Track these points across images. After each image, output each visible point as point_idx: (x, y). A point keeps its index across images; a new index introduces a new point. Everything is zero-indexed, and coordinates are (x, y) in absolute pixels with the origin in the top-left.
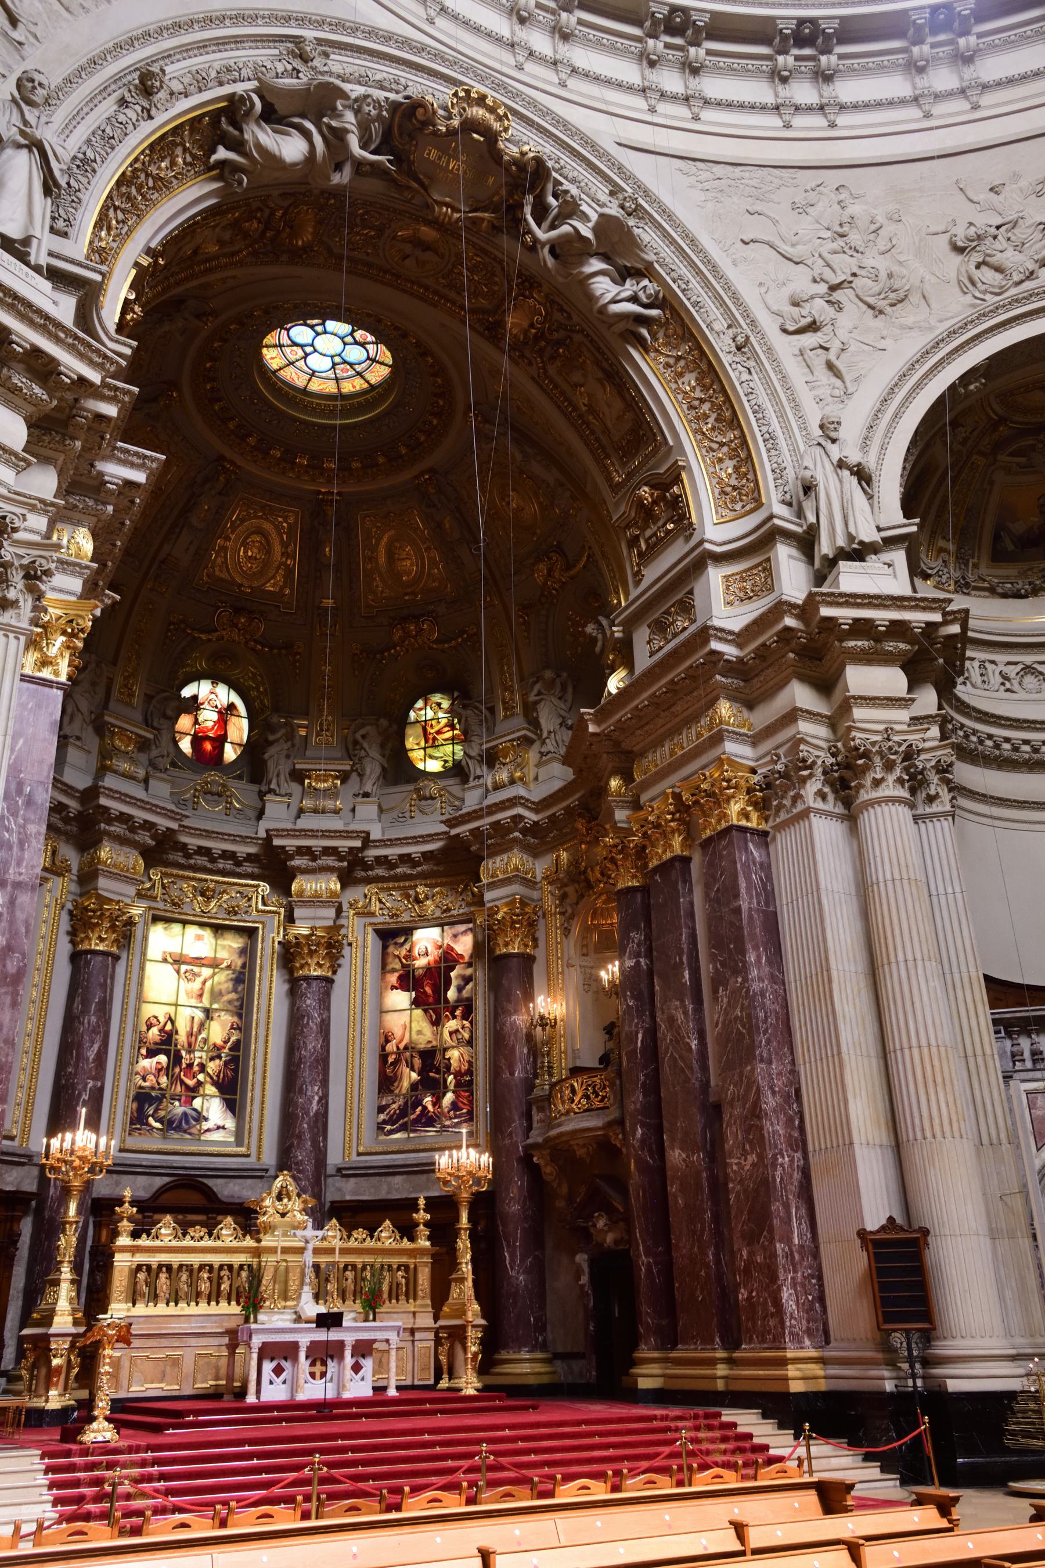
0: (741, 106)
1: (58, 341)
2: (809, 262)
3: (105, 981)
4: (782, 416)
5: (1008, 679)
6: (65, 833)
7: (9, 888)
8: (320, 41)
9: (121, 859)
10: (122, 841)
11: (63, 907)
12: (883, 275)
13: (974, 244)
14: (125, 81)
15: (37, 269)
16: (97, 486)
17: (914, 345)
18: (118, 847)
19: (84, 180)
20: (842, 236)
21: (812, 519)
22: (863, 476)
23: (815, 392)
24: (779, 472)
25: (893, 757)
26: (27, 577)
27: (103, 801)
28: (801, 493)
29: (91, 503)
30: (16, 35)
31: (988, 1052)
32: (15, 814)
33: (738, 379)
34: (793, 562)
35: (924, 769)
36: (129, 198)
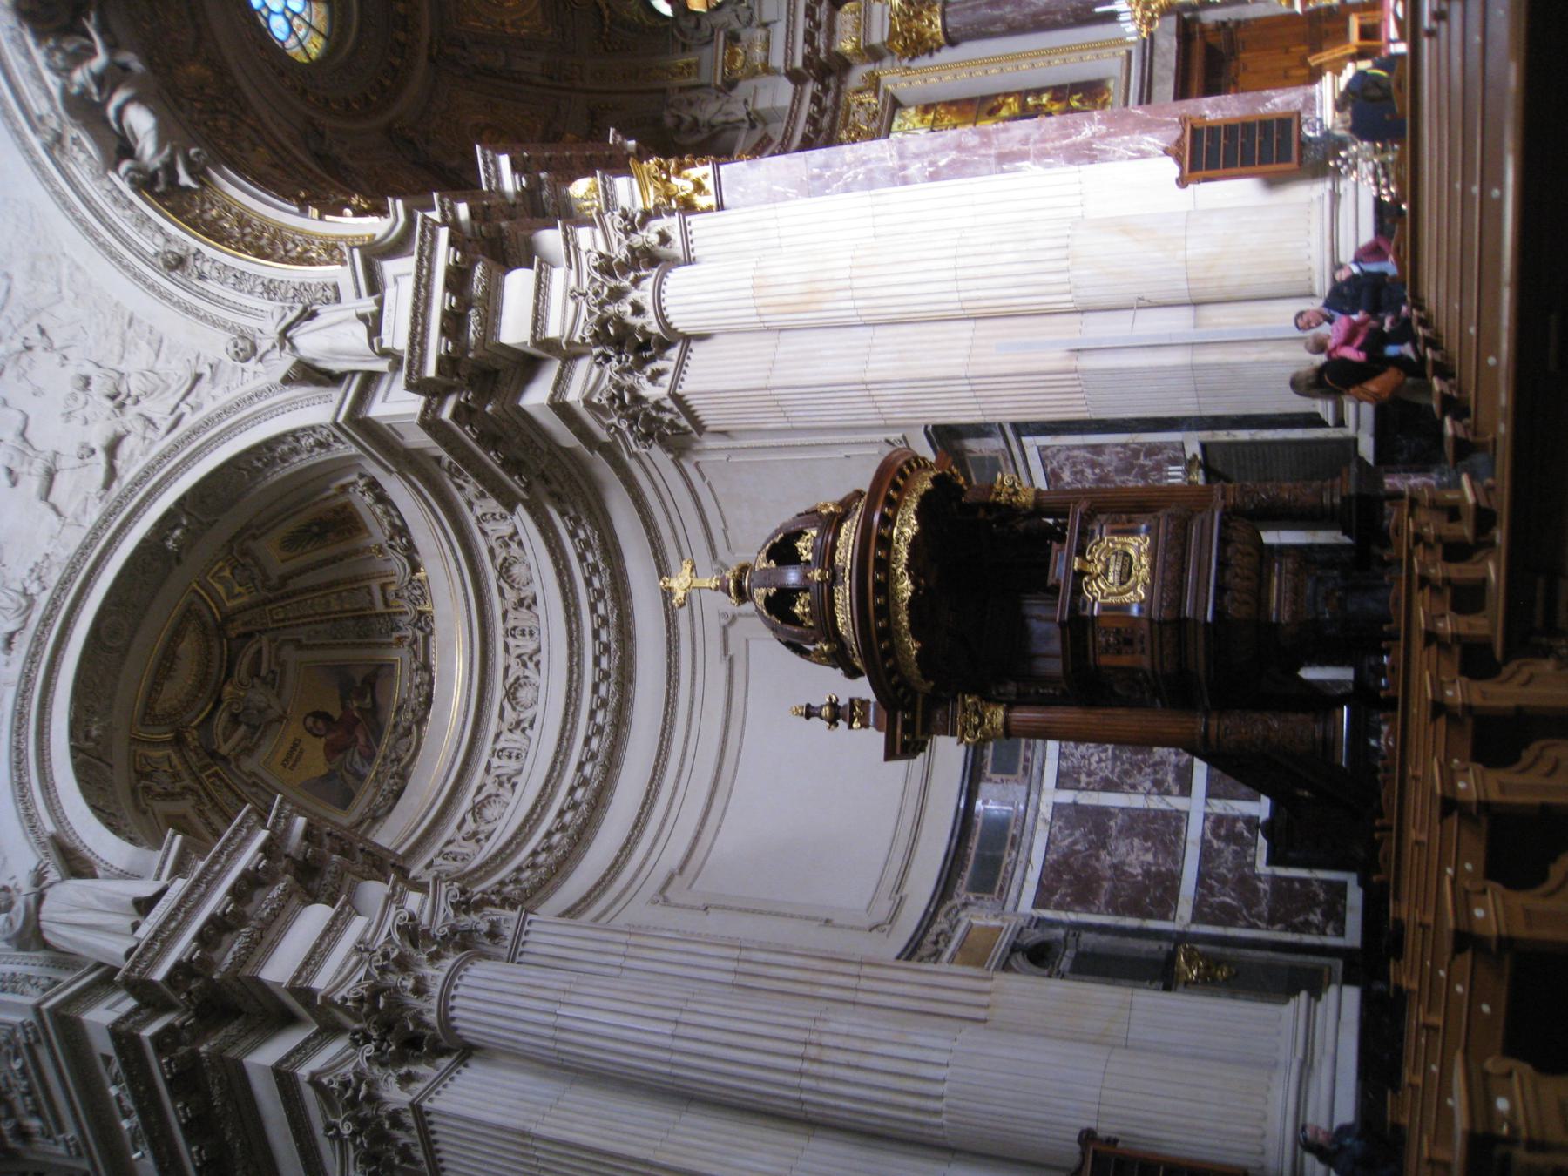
1: (431, 272)
3: (969, 8)
6: (838, 88)
7: (906, 162)
8: (35, 130)
9: (849, 28)
10: (831, 32)
11: (908, 68)
14: (184, 281)
15: (380, 303)
16: (530, 194)
18: (838, 36)
19: (283, 286)
26: (634, 231)
27: (799, 63)
29: (545, 193)
30: (207, 372)
32: (840, 175)
36: (272, 243)
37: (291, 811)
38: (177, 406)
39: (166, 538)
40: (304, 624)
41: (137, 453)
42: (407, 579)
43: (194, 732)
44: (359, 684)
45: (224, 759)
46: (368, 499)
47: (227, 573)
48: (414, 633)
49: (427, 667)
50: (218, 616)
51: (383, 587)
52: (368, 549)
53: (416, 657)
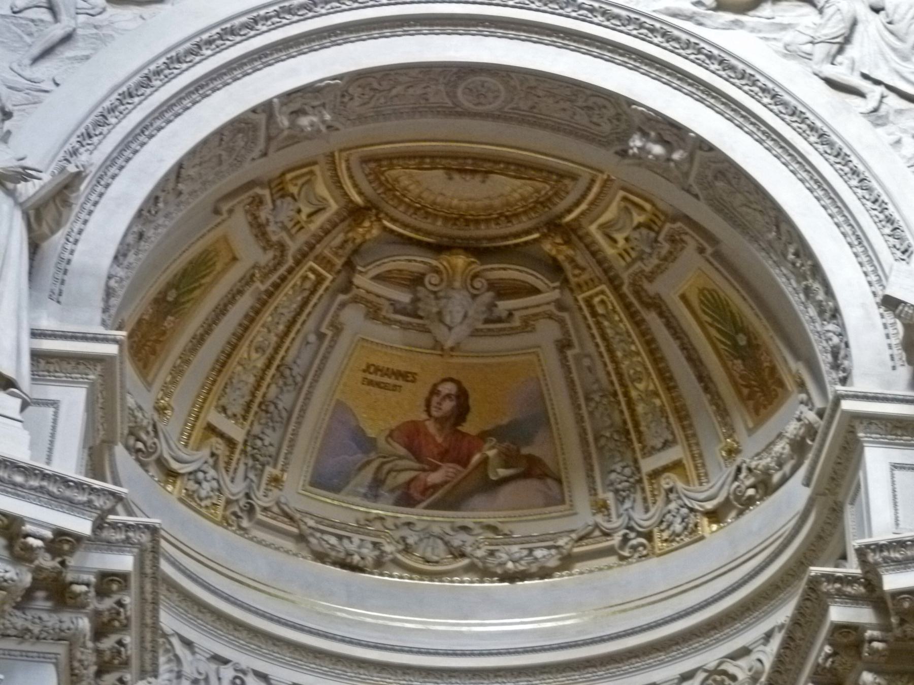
37: (140, 544)
38: (877, 82)
39: (645, 134)
40: (597, 345)
41: (788, 36)
42: (696, 506)
43: (375, 232)
44: (525, 451)
45: (347, 287)
46: (792, 428)
47: (638, 218)
48: (615, 530)
49: (567, 562)
50: (569, 218)
51: (676, 466)
52: (731, 431)
53: (581, 538)
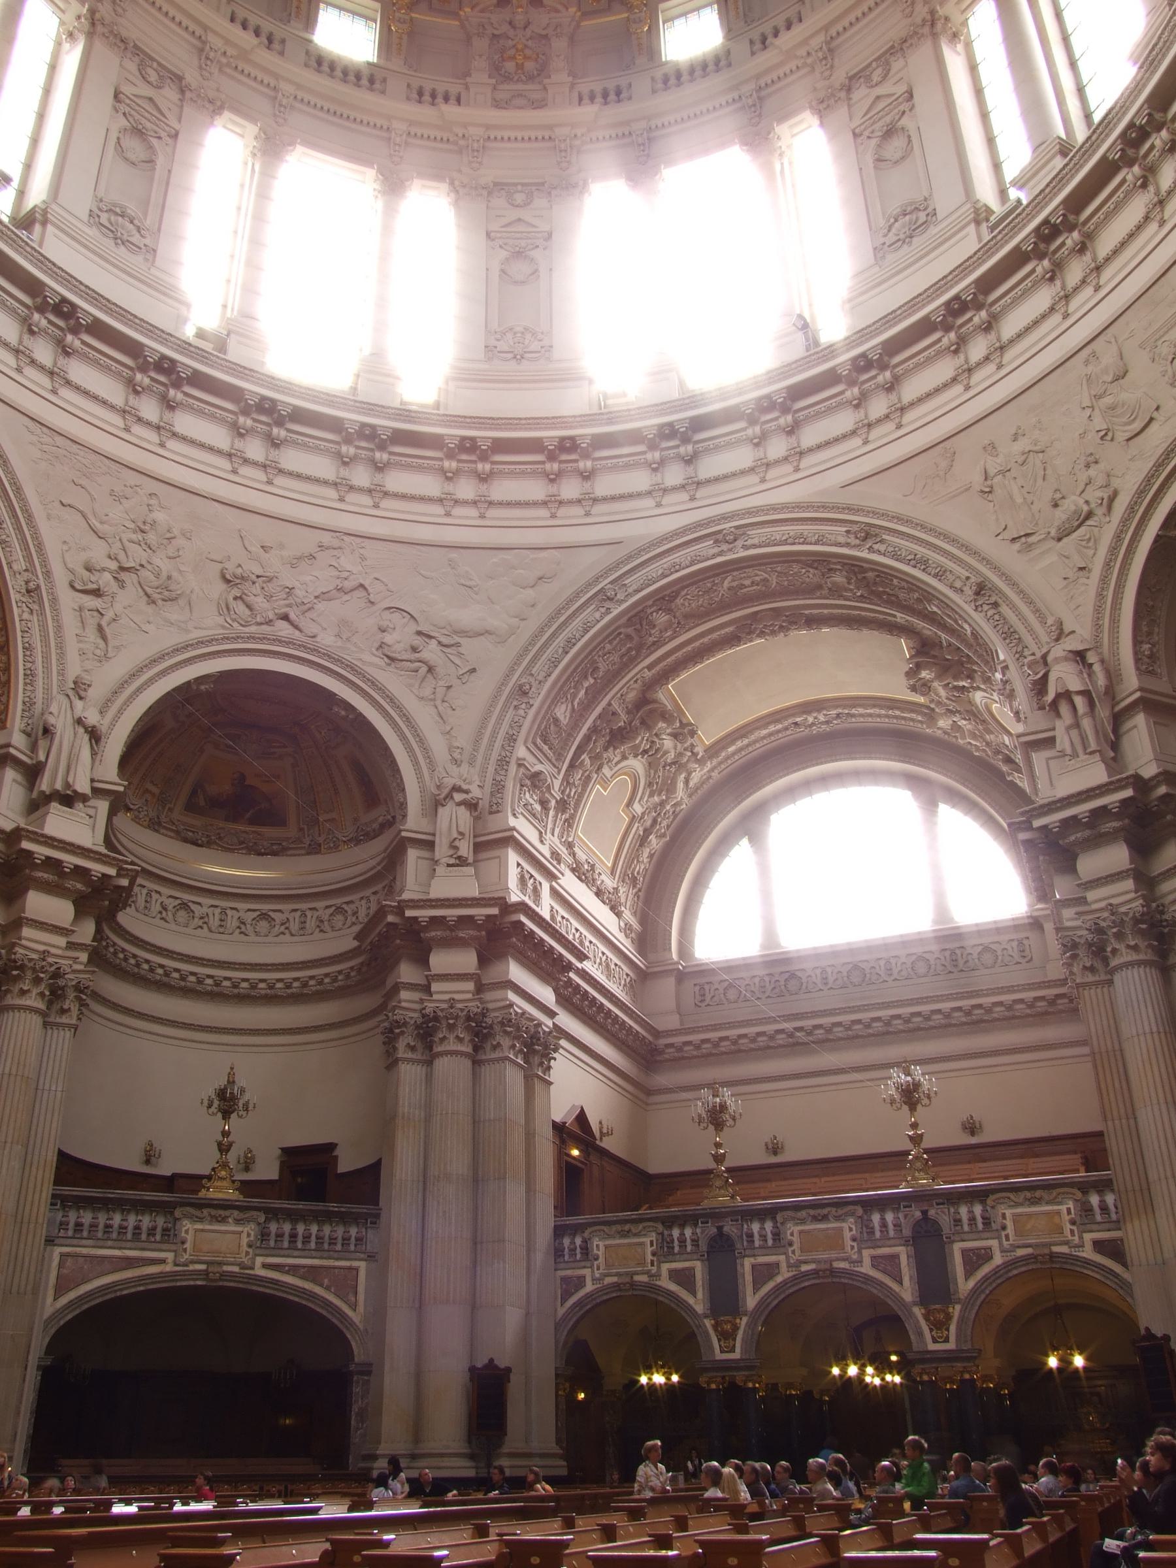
0: (95, 398)
2: (110, 541)
4: (46, 658)
5: (165, 909)
12: (164, 575)
13: (238, 581)
17: (173, 638)
20: (143, 532)
21: (42, 758)
22: (95, 736)
23: (81, 645)
24: (29, 705)
25: (42, 975)
28: (40, 732)
31: (40, 1221)
33: (20, 616)
34: (15, 786)
35: (66, 986)
